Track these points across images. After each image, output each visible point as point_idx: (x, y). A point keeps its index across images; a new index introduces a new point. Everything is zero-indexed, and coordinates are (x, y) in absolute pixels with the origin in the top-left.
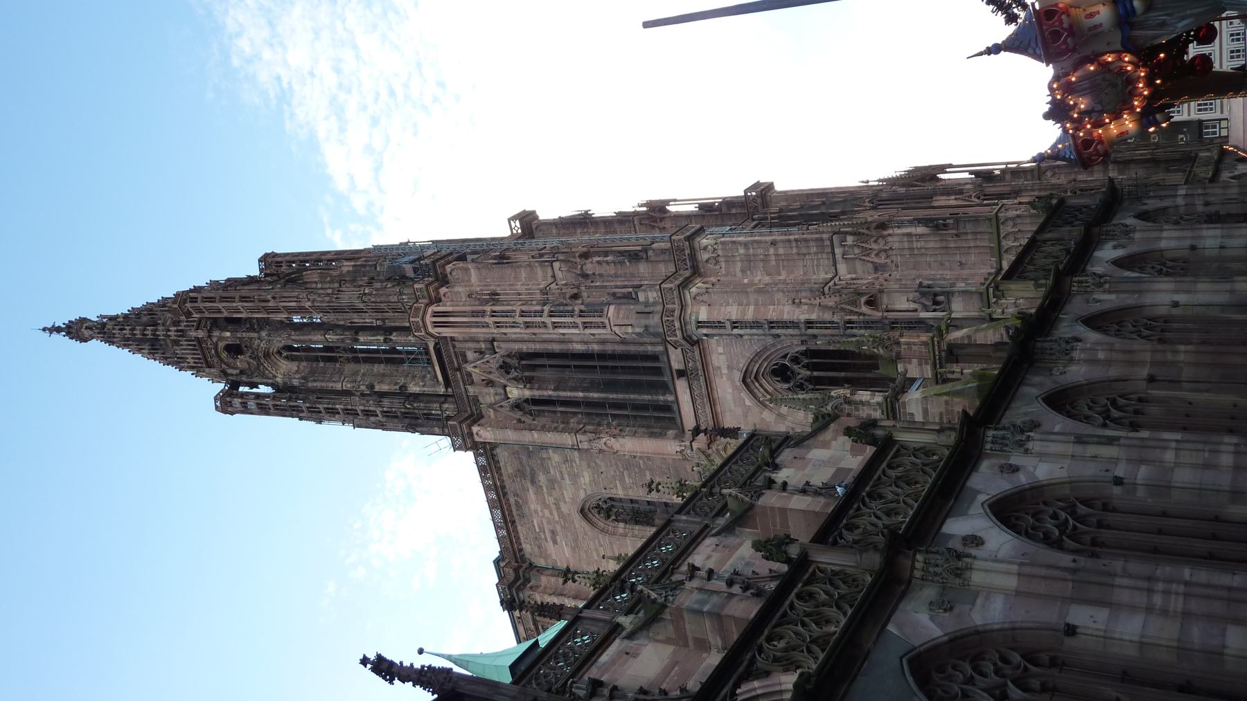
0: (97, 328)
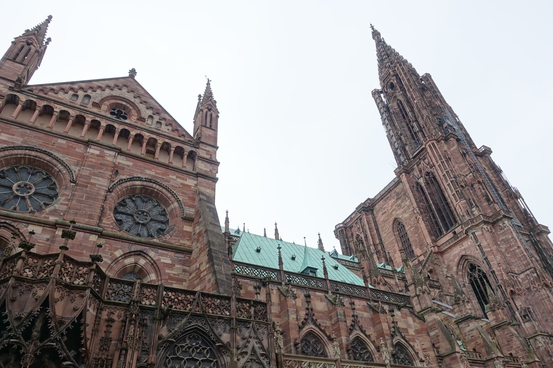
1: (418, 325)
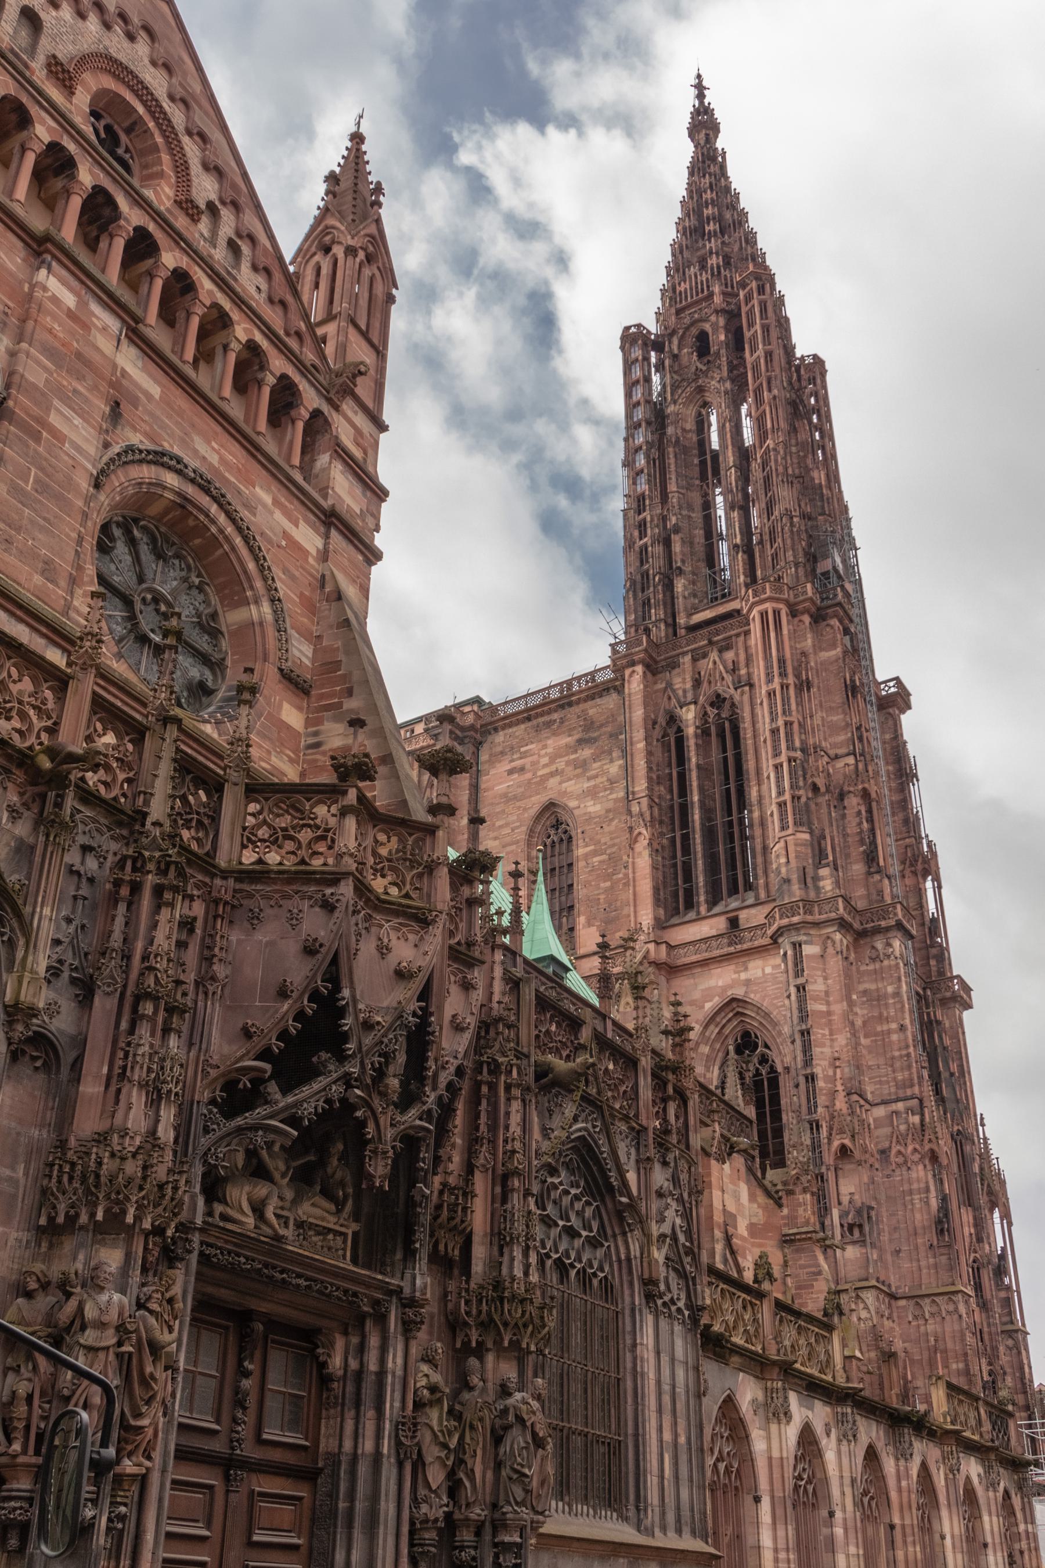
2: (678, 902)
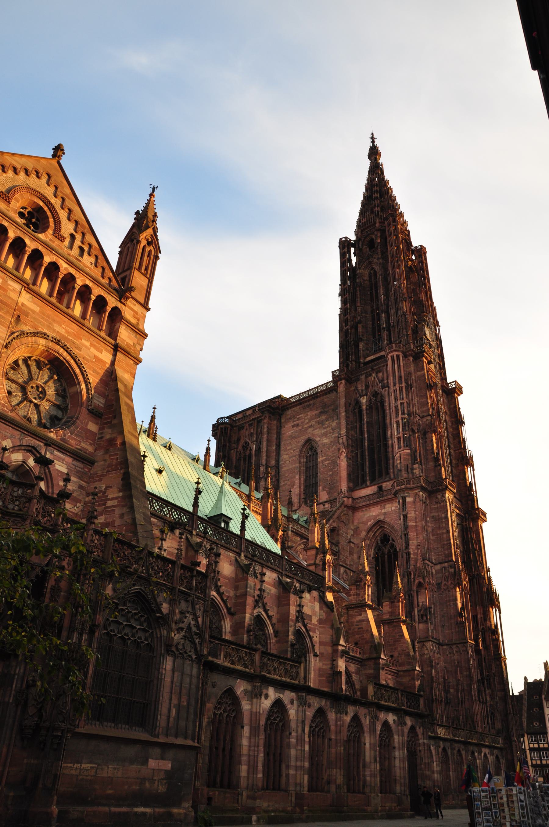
0: (376, 163)
1: (324, 614)
2: (358, 480)
